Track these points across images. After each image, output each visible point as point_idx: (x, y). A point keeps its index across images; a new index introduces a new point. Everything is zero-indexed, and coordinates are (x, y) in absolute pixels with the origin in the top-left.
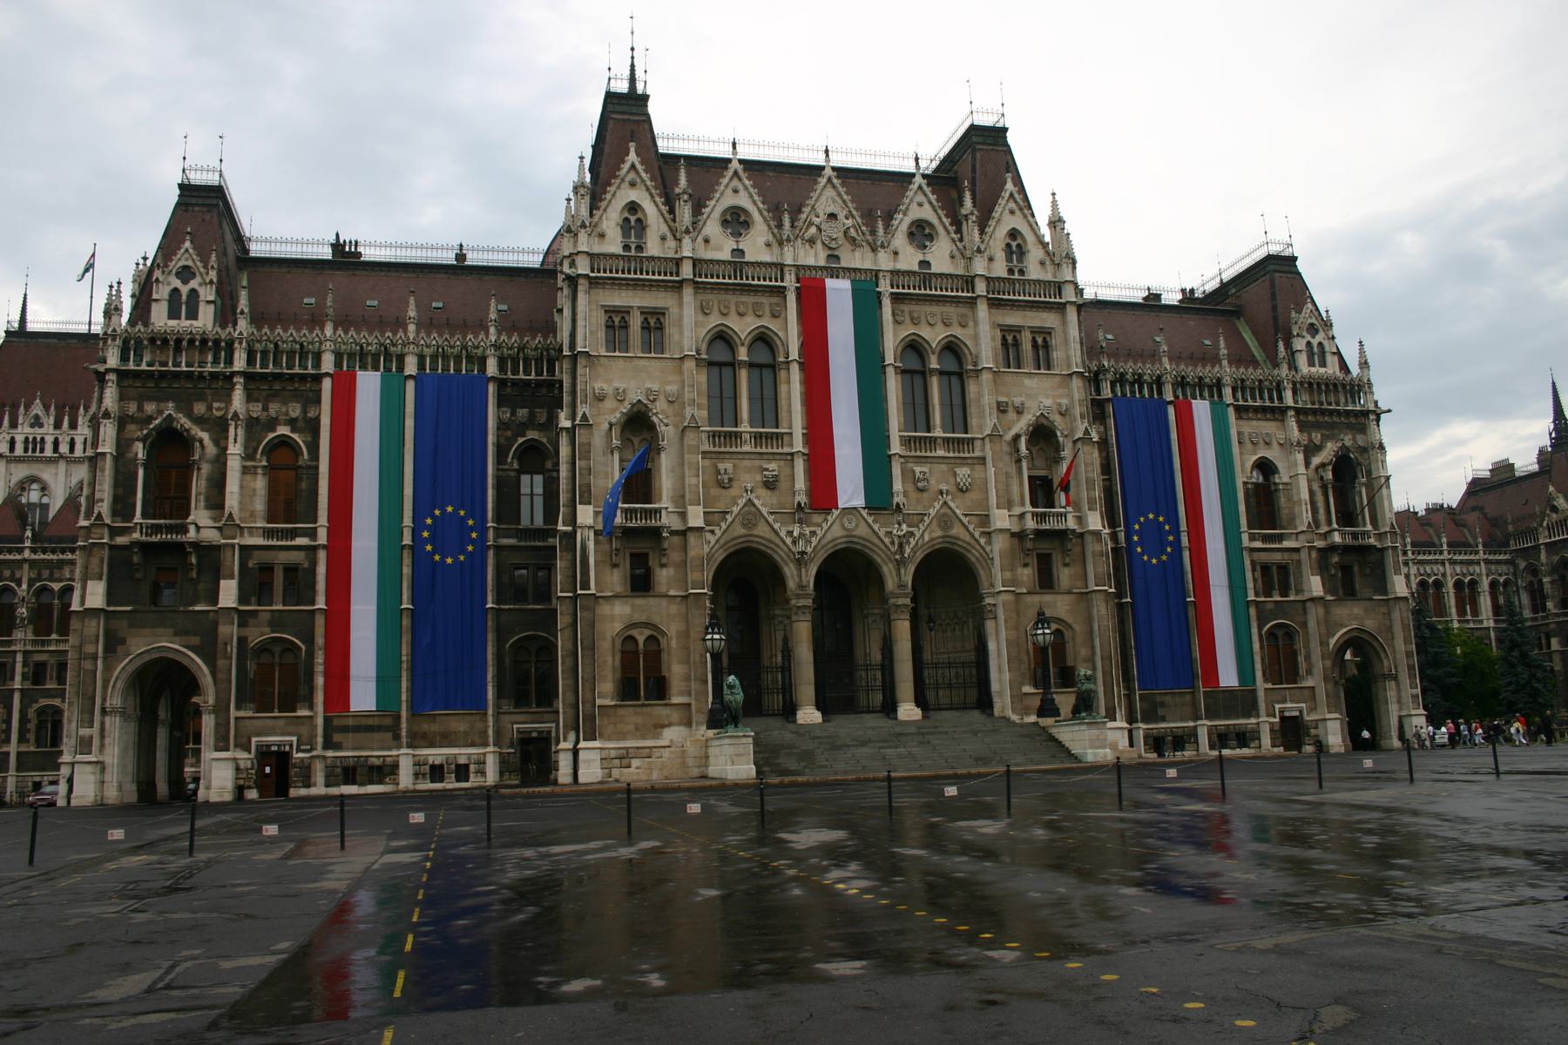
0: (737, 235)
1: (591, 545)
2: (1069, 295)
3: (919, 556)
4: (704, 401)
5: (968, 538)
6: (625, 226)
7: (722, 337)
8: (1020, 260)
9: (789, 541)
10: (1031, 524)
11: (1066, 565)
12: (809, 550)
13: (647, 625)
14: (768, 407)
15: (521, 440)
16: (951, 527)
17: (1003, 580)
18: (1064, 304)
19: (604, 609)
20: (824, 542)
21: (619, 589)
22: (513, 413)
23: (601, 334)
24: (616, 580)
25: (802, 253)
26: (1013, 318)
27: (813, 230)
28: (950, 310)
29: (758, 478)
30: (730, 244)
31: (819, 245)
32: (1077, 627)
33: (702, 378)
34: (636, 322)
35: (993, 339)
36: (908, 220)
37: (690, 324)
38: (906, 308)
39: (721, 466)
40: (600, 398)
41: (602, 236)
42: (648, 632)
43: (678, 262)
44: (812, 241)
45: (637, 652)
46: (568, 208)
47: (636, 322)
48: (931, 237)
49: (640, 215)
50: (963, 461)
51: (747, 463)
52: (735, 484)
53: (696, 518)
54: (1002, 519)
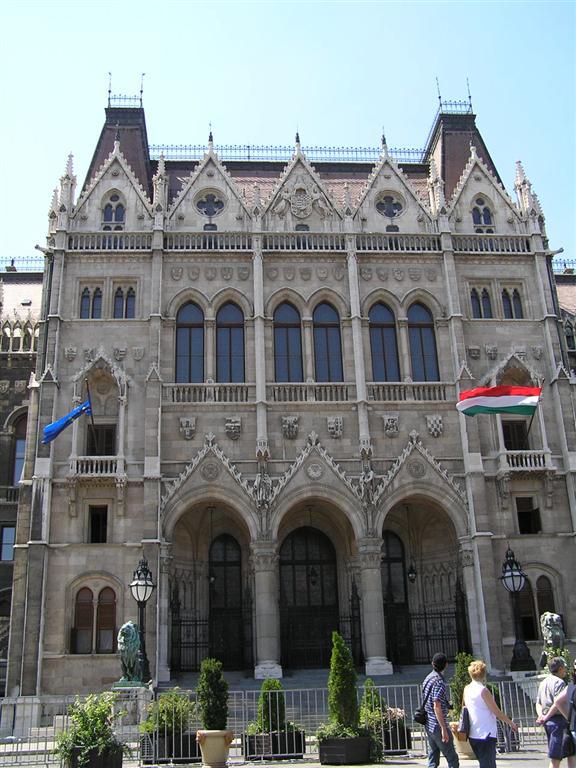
0: (210, 213)
1: (46, 496)
2: (536, 246)
3: (390, 504)
4: (171, 359)
5: (441, 484)
6: (107, 212)
7: (190, 304)
8: (488, 220)
9: (250, 491)
10: (505, 467)
11: (551, 508)
12: (271, 499)
13: (103, 573)
14: (232, 365)
15: (16, 408)
16: (424, 473)
17: (478, 528)
18: (533, 256)
19: (60, 560)
20: (287, 491)
21: (75, 539)
22: (12, 385)
23: (75, 303)
24: (75, 528)
25: (272, 224)
26: (483, 271)
27: (283, 203)
28: (417, 265)
29: (222, 430)
30: (205, 220)
31: (289, 216)
32: (563, 573)
33: (170, 338)
34: (108, 293)
35: (461, 291)
36: (375, 192)
37: (156, 290)
38: (373, 265)
39: (183, 420)
40: (71, 359)
41: (84, 219)
42: (103, 584)
43: (150, 236)
44: (282, 214)
45: (91, 605)
46: (55, 197)
47: (108, 293)
48: (398, 206)
49: (120, 201)
50: (435, 409)
51: (210, 416)
52: (198, 437)
53: (153, 468)
54: (473, 463)
